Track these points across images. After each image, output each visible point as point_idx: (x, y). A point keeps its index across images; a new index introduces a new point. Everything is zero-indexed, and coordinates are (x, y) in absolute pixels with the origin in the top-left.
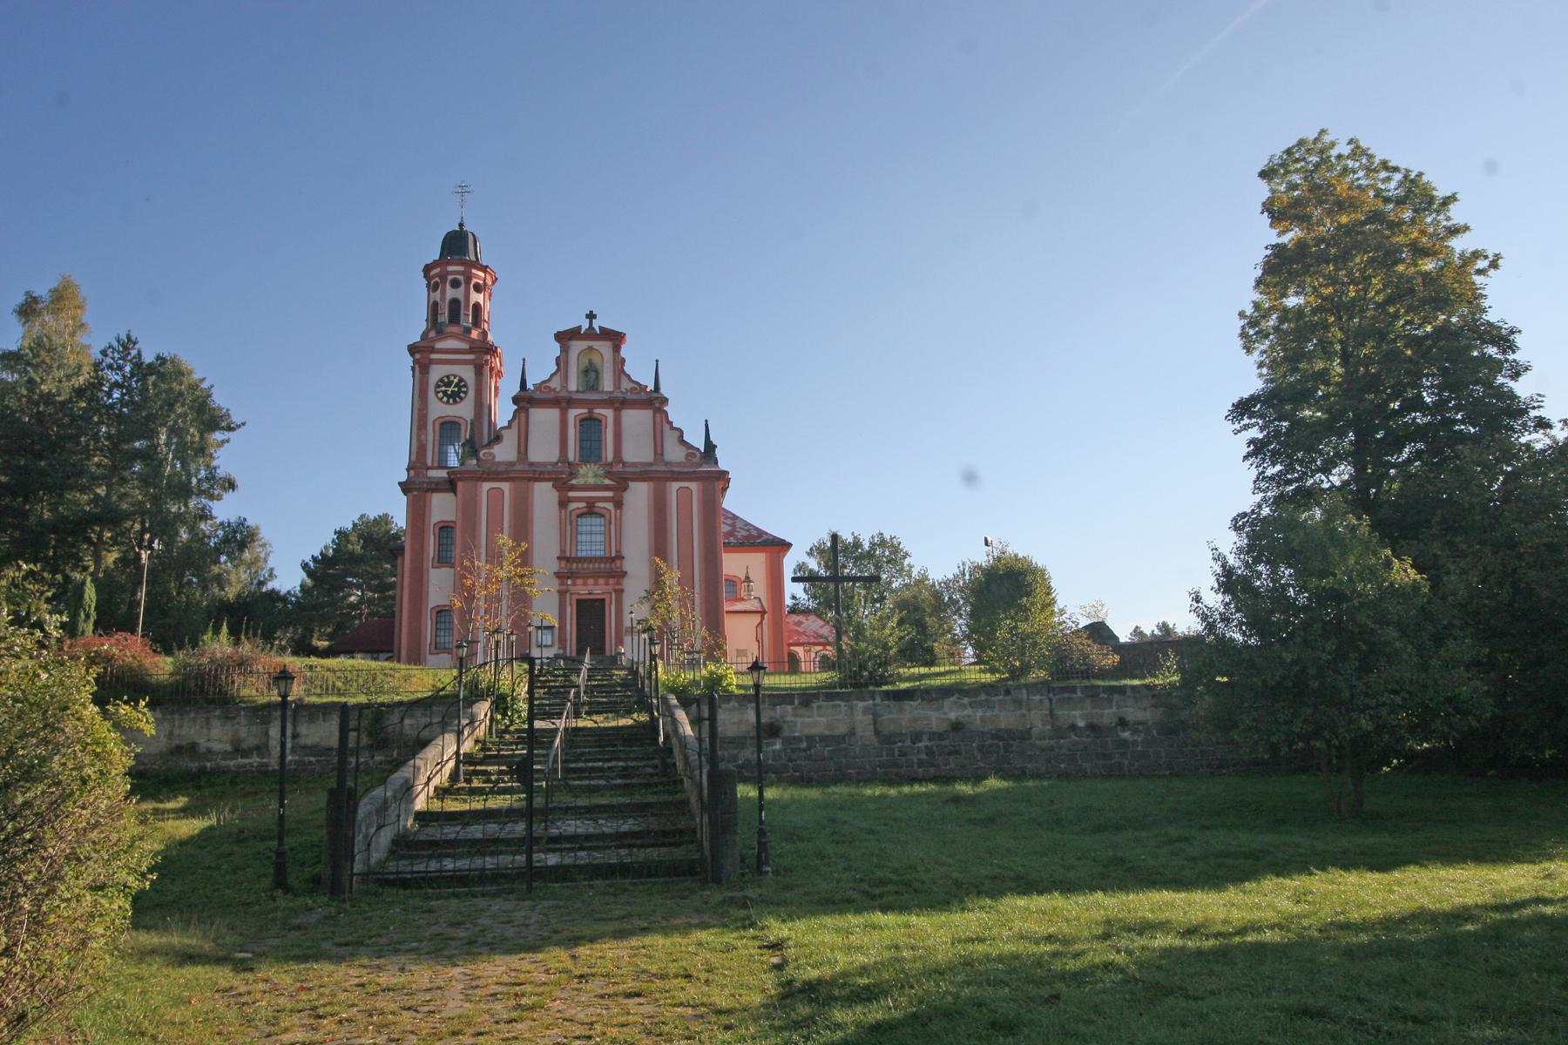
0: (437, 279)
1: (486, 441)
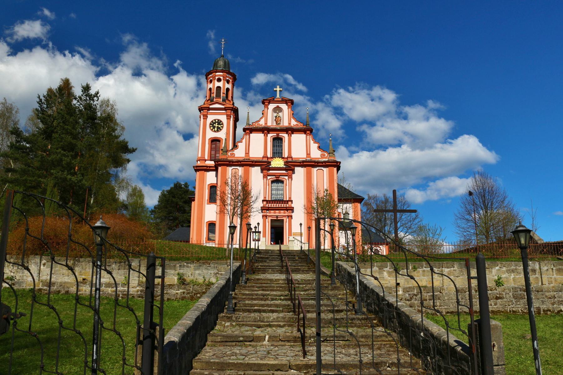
1: (230, 148)
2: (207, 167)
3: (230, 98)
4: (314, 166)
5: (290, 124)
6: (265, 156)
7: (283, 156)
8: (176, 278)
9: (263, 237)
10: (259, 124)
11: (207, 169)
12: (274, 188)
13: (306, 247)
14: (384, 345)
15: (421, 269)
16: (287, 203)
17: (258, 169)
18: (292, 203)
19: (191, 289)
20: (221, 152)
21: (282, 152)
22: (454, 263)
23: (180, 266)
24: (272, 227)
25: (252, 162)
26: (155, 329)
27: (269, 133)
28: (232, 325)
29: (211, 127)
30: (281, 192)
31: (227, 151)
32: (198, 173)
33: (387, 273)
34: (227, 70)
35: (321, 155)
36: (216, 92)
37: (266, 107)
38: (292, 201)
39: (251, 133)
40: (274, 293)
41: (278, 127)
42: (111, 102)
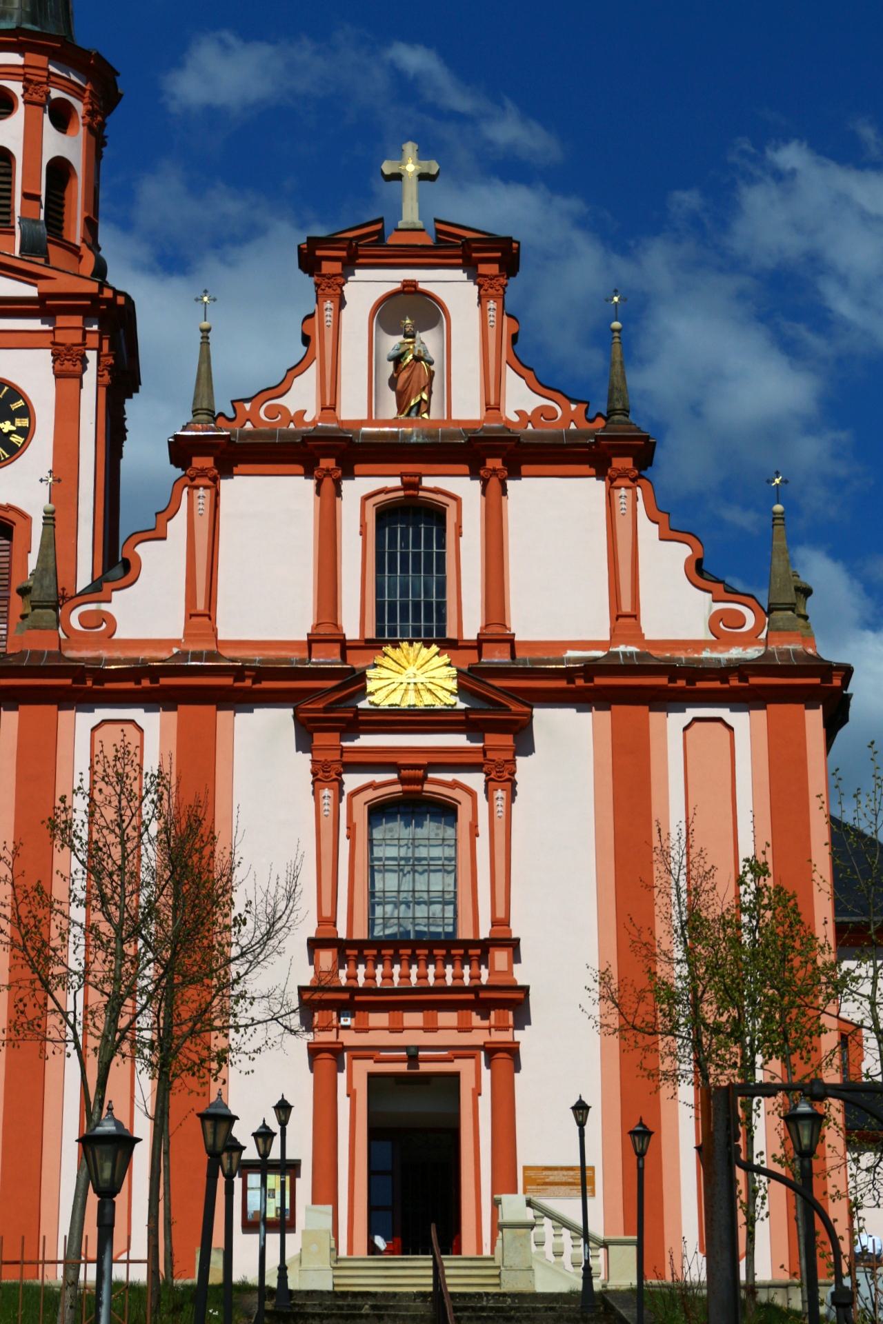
1: (84, 579)
3: (76, 232)
5: (493, 406)
6: (325, 630)
7: (451, 633)
10: (283, 410)
12: (392, 852)
16: (484, 959)
18: (516, 958)
20: (18, 605)
21: (442, 606)
25: (238, 672)
27: (350, 475)
30: (437, 882)
31: (60, 600)
34: (51, 30)
35: (715, 621)
38: (513, 945)
39: (227, 472)
41: (412, 432)
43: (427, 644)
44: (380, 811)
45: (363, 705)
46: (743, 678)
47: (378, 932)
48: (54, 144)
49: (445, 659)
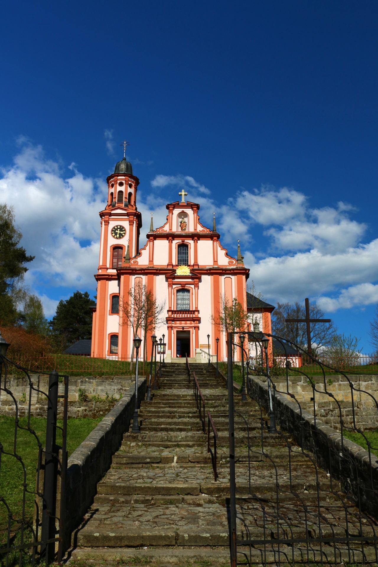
0: (113, 183)
1: (133, 256)
2: (109, 275)
3: (132, 203)
4: (221, 274)
5: (195, 230)
7: (189, 264)
8: (77, 395)
9: (168, 349)
10: (164, 230)
11: (109, 278)
12: (180, 297)
13: (214, 360)
14: (300, 465)
15: (337, 383)
16: (194, 313)
17: (163, 277)
18: (199, 313)
19: (93, 406)
20: (124, 260)
21: (188, 260)
22: (371, 377)
23: (82, 382)
24: (178, 339)
25: (157, 270)
26: (57, 453)
27: (174, 240)
28: (137, 445)
29: (112, 233)
30: (187, 302)
31: (130, 259)
32: (99, 282)
33: (301, 387)
34: (129, 173)
35: (229, 262)
36: (118, 197)
37: (171, 212)
38: (198, 311)
39: (155, 239)
40: (182, 410)
41: (183, 233)
42: (8, 208)
43: (185, 266)
44: (178, 291)
45: (176, 275)
46: (233, 271)
47: (178, 309)
48: (130, 190)
49: (188, 268)
